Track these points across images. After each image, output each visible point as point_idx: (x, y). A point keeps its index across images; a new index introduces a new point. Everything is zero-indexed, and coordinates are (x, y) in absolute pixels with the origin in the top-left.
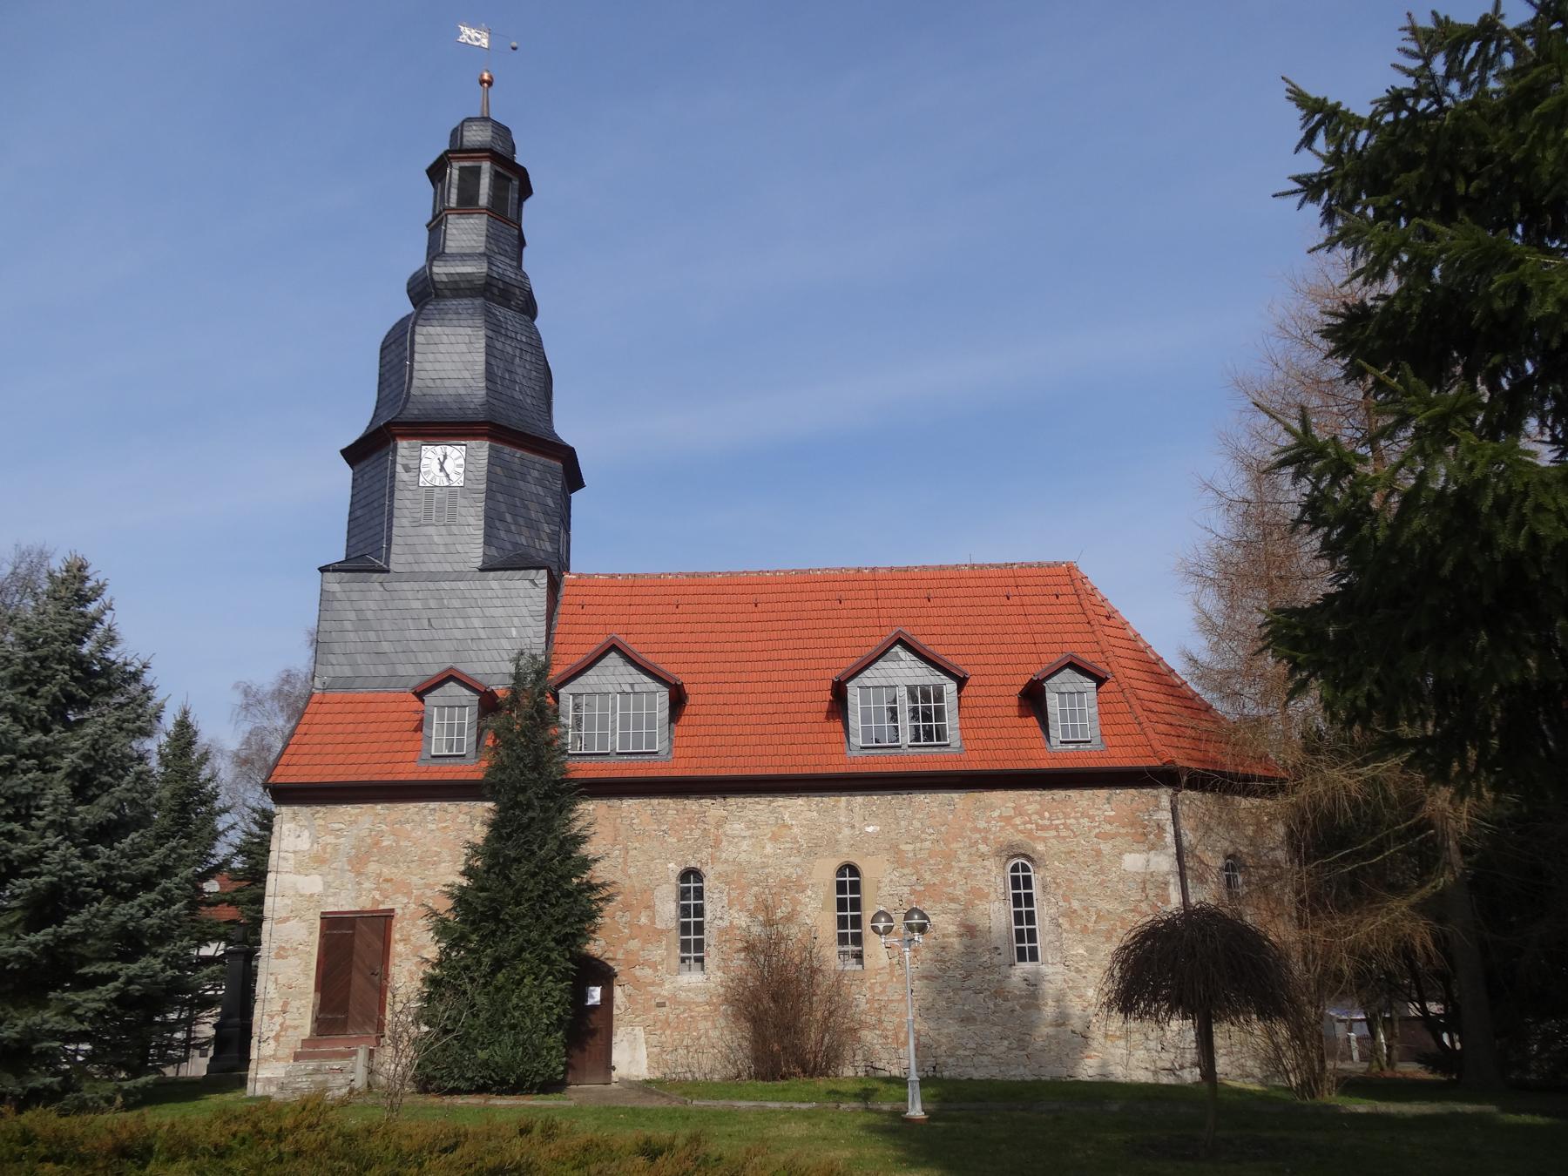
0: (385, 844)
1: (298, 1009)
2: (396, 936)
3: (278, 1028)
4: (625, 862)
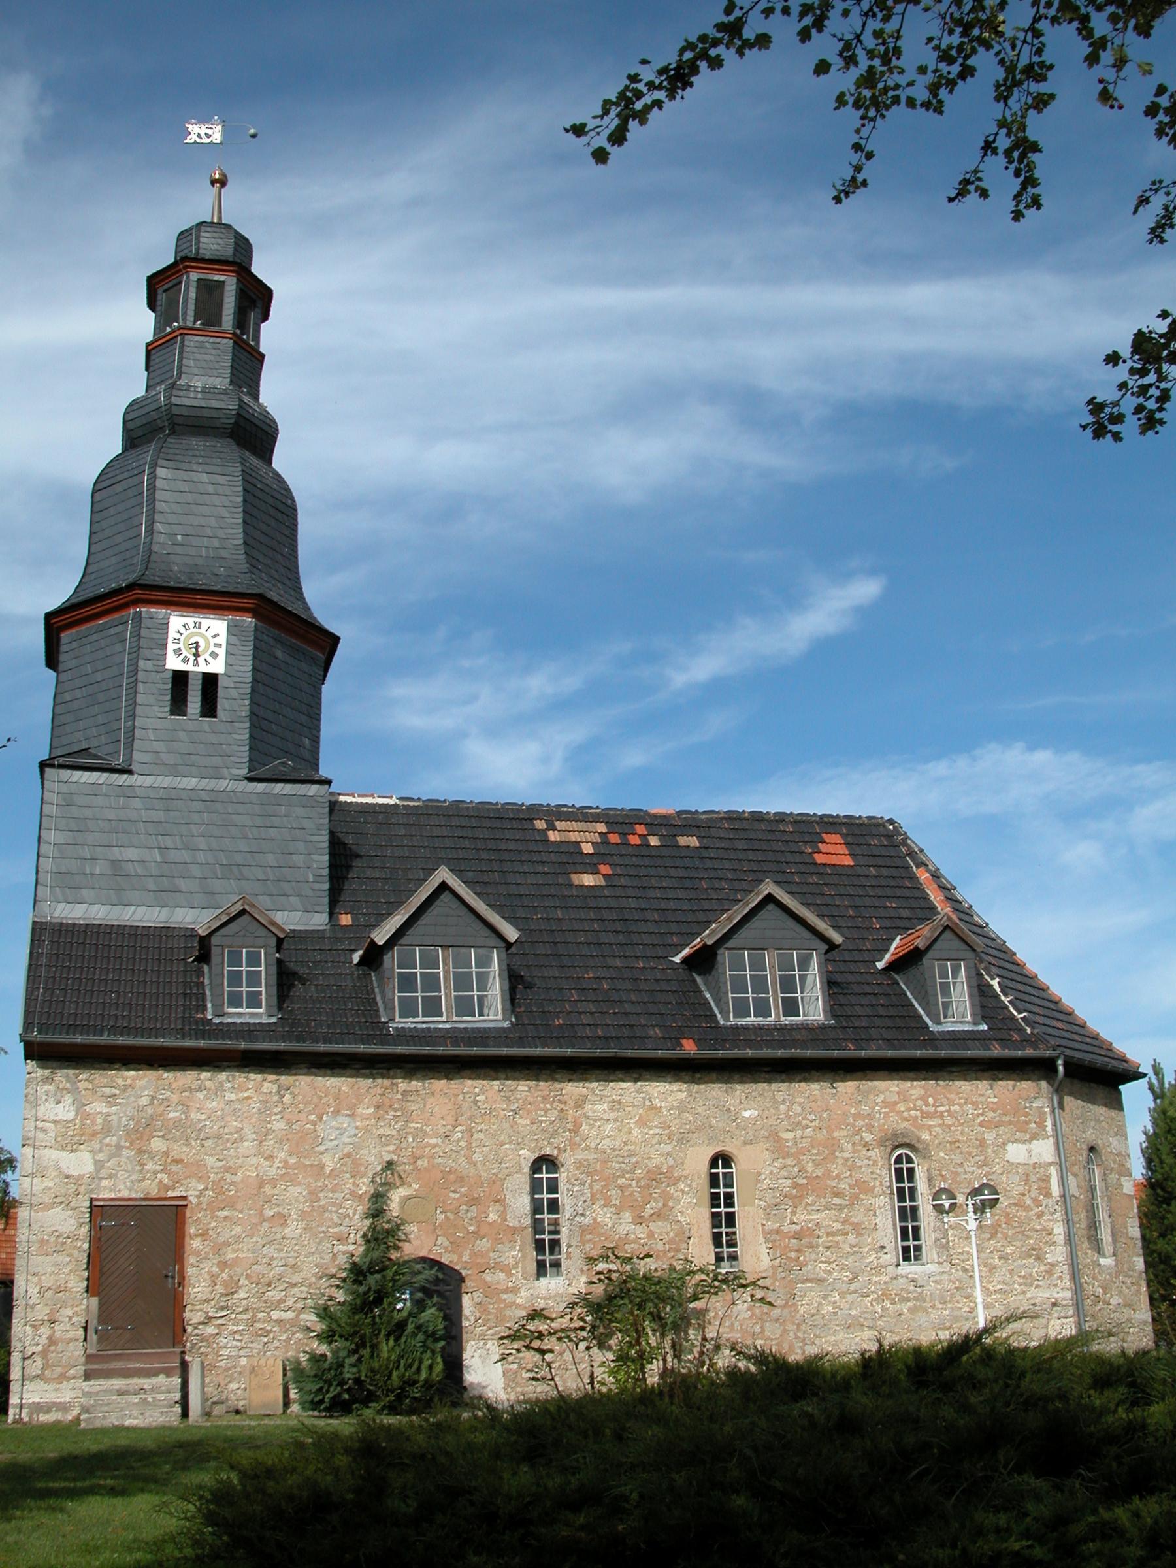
0: (171, 1115)
1: (70, 1318)
2: (191, 1230)
3: (44, 1340)
4: (469, 1147)
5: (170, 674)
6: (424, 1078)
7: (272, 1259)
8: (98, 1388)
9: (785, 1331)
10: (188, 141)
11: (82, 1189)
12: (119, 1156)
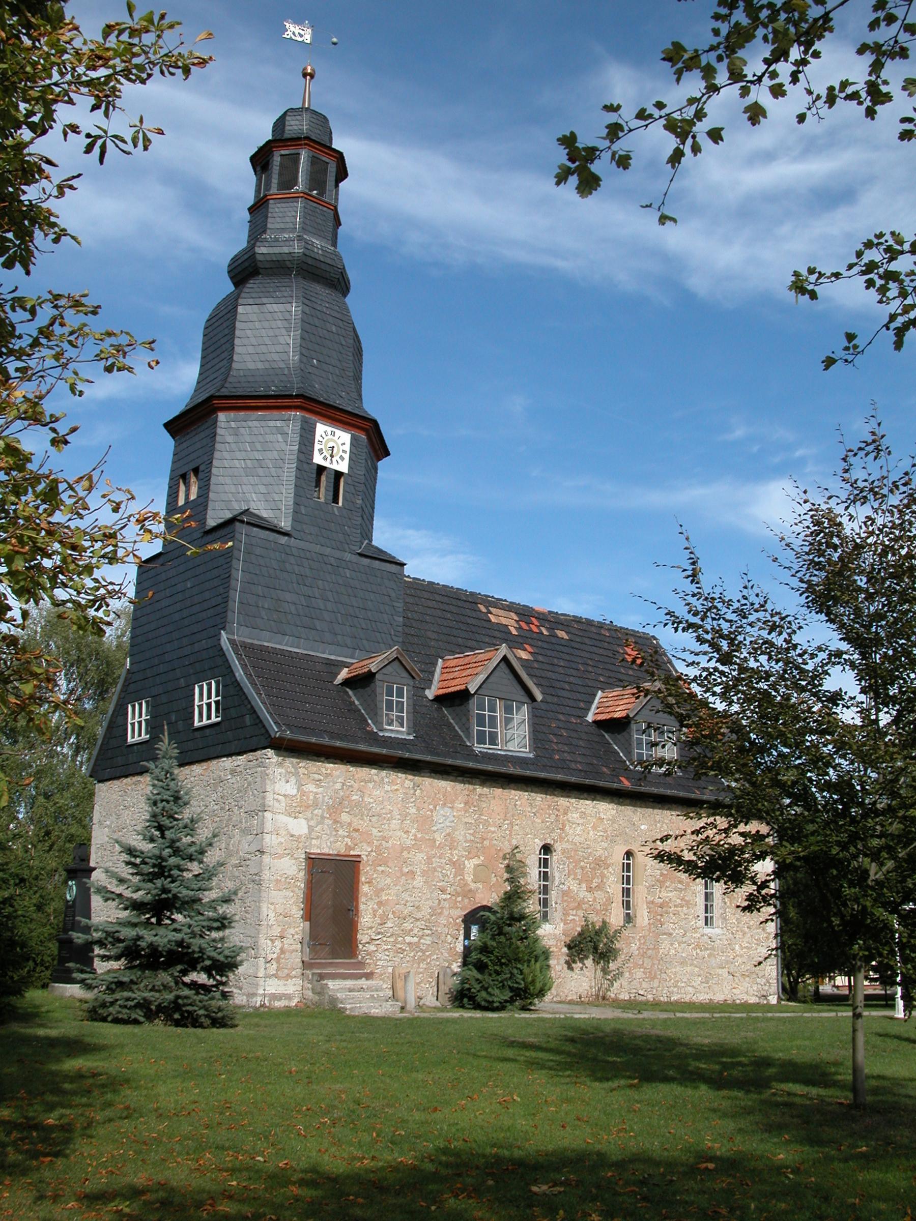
0: (354, 797)
1: (293, 935)
2: (363, 879)
3: (277, 950)
4: (511, 835)
5: (315, 468)
6: (490, 786)
7: (407, 901)
8: (338, 987)
9: (653, 964)
10: (285, 36)
11: (301, 845)
12: (323, 823)
